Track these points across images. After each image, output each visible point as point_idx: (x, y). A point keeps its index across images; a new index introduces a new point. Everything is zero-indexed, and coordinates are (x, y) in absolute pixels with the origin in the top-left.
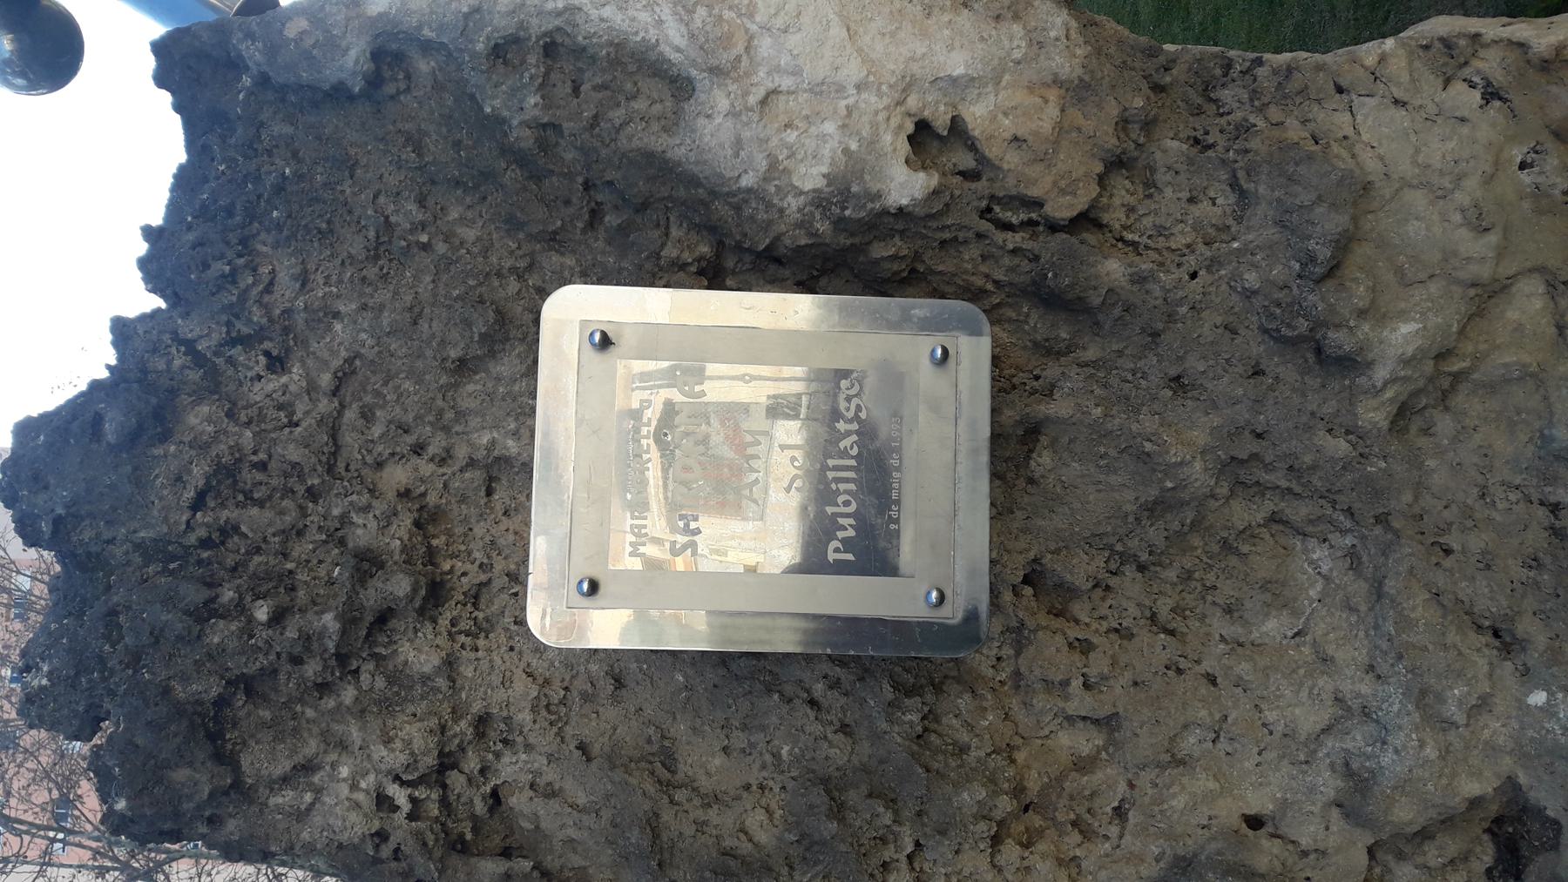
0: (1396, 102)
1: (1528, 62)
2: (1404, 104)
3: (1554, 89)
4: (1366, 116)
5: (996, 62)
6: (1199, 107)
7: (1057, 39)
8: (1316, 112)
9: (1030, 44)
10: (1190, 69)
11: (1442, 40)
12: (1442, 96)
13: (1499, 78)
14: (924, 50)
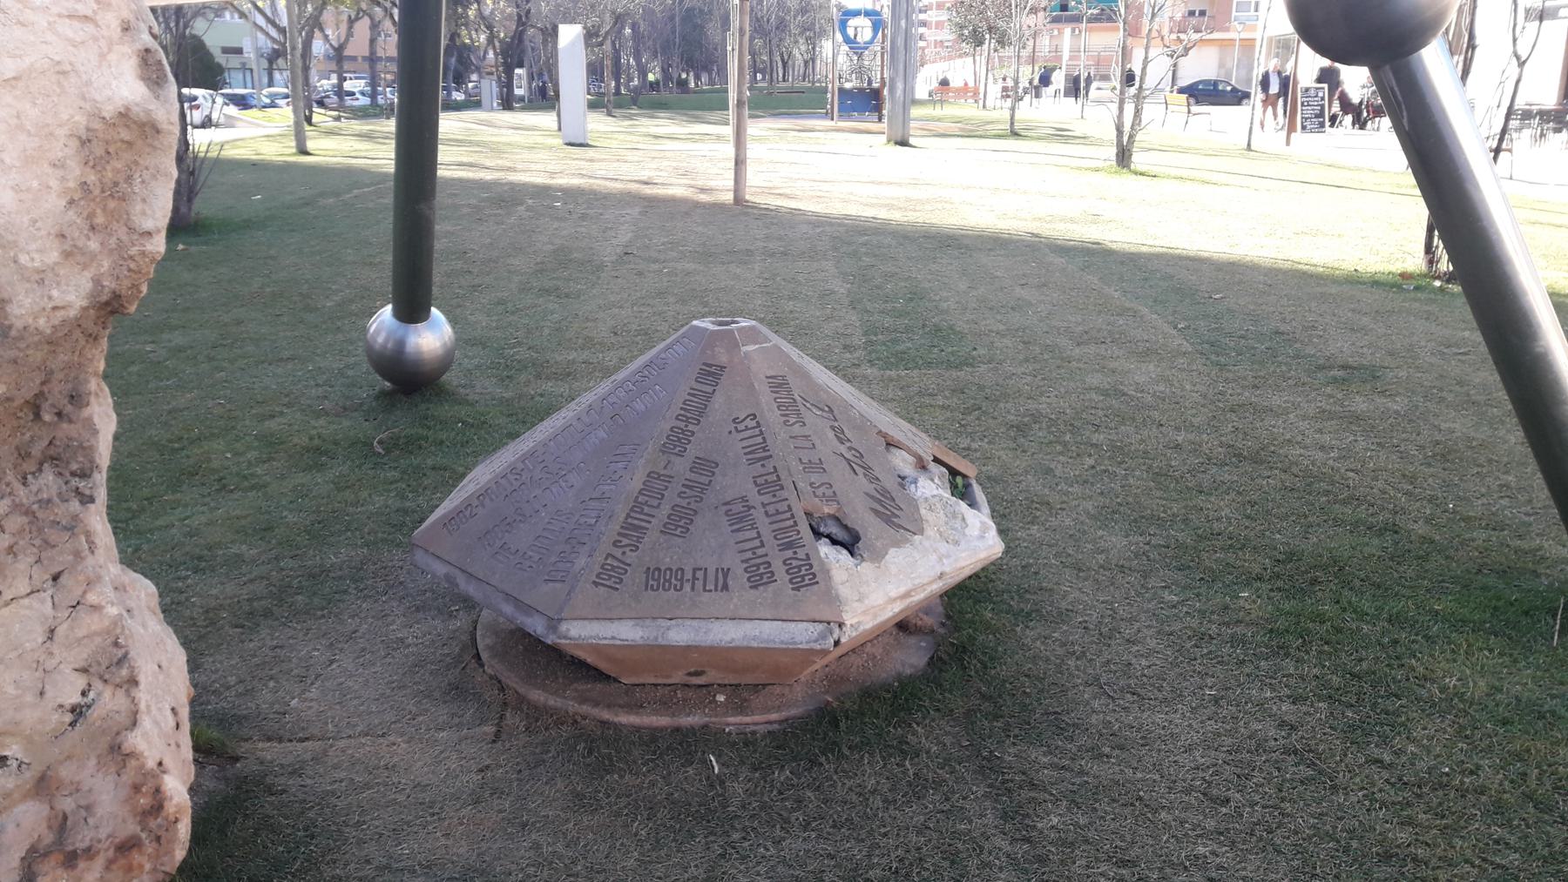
0: (52, 631)
1: (118, 733)
2: (50, 639)
3: (93, 762)
4: (30, 607)
5: (10, 238)
6: (29, 455)
7: (50, 298)
8: (24, 562)
9: (38, 271)
10: (70, 439)
11: (126, 655)
12: (67, 669)
13: (94, 714)
14: (8, 161)
